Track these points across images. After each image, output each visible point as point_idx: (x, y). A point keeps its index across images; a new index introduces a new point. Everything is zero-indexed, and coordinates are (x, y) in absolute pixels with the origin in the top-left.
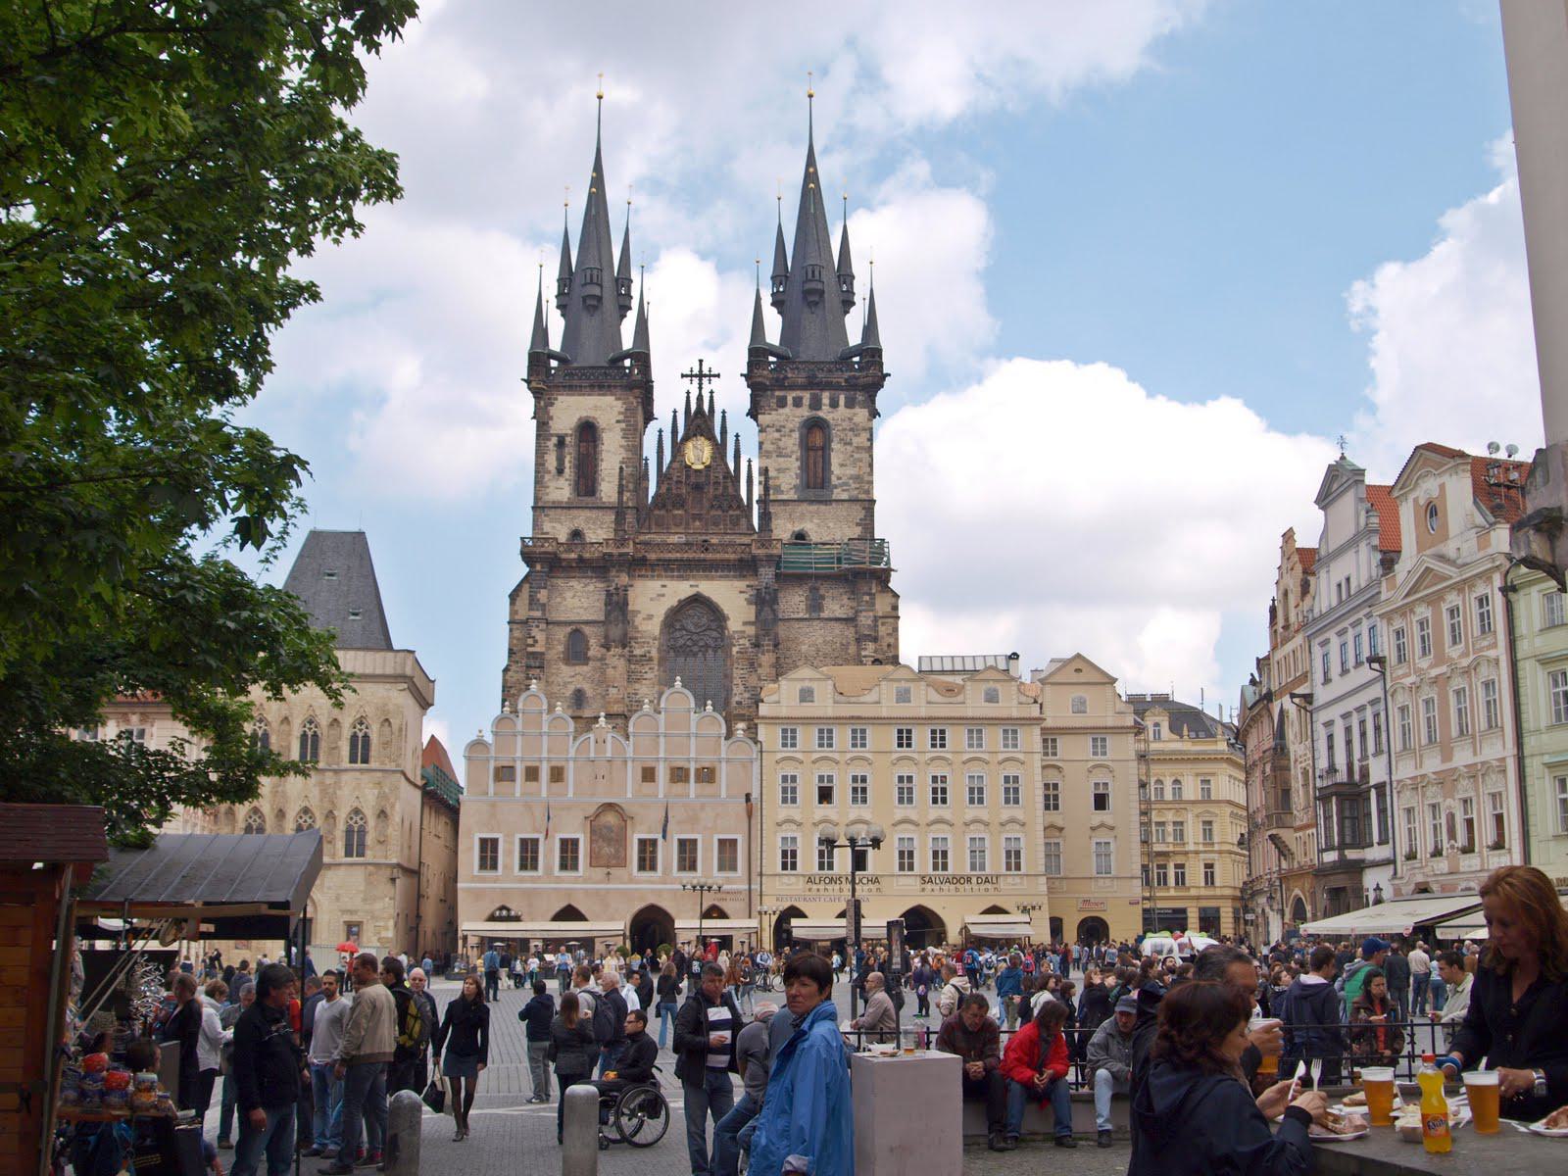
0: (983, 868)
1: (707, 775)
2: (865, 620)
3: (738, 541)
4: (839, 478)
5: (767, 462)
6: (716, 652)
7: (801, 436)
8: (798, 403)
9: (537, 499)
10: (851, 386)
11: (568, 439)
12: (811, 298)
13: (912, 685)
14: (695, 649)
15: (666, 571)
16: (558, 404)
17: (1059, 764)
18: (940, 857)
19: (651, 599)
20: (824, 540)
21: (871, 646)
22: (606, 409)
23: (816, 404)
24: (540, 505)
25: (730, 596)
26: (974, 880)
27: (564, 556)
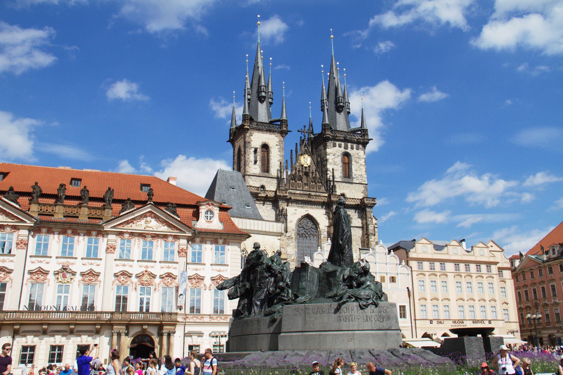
2: (371, 227)
3: (321, 195)
4: (355, 175)
5: (331, 166)
7: (342, 157)
8: (340, 146)
10: (358, 143)
11: (258, 150)
14: (307, 235)
15: (296, 204)
19: (291, 215)
21: (373, 237)
22: (272, 140)
23: (346, 148)
24: (248, 174)
27: (259, 195)
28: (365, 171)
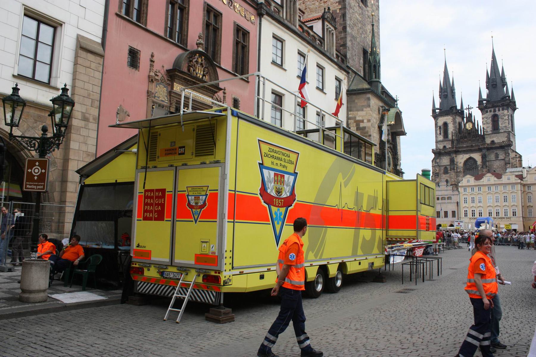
0: (507, 216)
1: (449, 198)
2: (507, 159)
6: (476, 168)
7: (492, 119)
8: (490, 111)
9: (436, 140)
10: (503, 105)
12: (495, 86)
13: (490, 177)
16: (439, 120)
17: (531, 192)
18: (498, 213)
20: (499, 142)
22: (448, 119)
25: (477, 157)
26: (505, 218)
28: (509, 123)
